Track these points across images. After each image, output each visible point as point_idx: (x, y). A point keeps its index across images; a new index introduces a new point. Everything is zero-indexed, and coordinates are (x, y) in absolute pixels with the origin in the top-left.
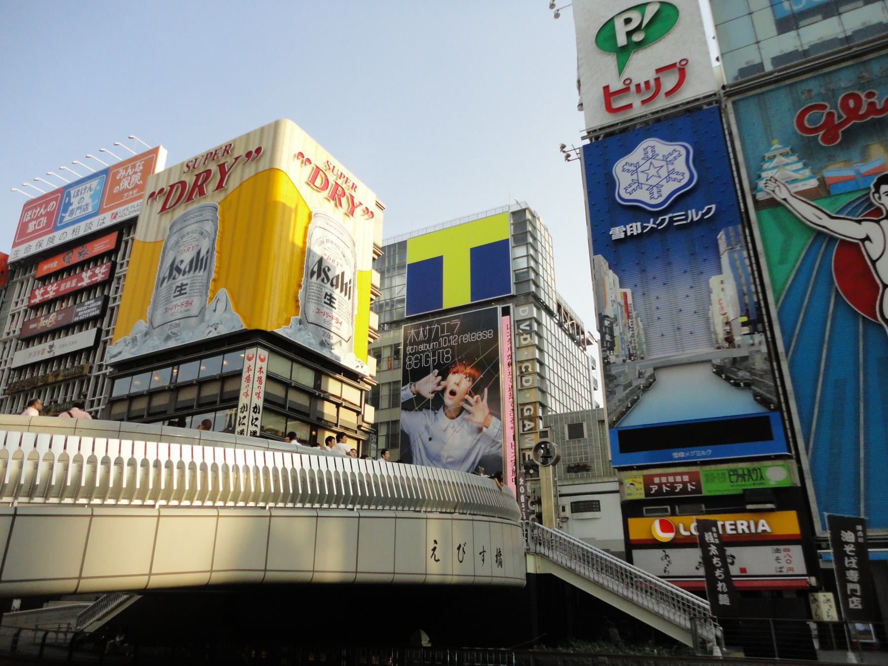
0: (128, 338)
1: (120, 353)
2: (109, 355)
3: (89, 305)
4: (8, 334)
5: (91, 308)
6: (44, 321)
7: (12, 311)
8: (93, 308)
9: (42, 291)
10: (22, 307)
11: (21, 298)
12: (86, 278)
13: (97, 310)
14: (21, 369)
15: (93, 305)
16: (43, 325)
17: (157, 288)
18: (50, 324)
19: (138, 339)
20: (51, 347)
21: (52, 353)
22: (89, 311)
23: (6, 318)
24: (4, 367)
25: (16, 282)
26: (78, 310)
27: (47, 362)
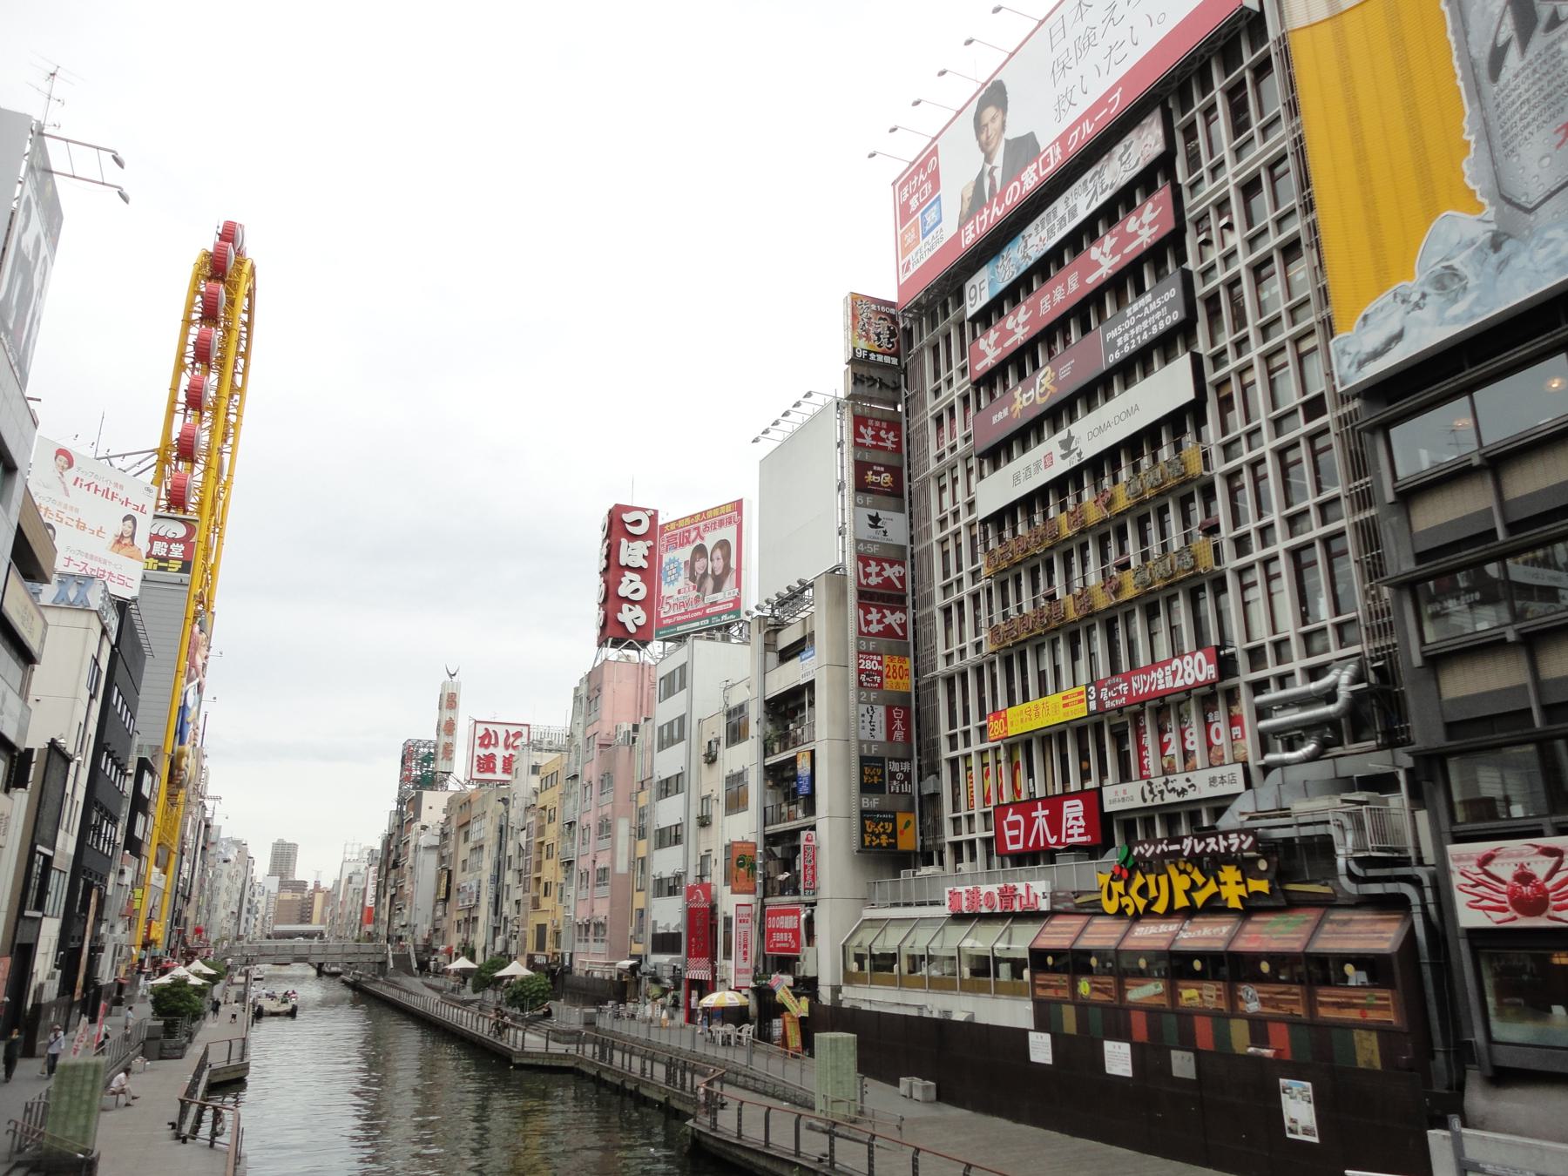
0: (1414, 284)
1: (1398, 337)
2: (1346, 360)
3: (1141, 310)
4: (940, 457)
5: (1148, 316)
6: (1025, 396)
7: (932, 409)
8: (1154, 312)
9: (993, 335)
10: (961, 385)
11: (944, 375)
12: (1104, 258)
13: (1170, 313)
14: (999, 519)
15: (1153, 307)
16: (1025, 404)
17: (1477, 92)
18: (1042, 395)
19: (1464, 270)
20: (1066, 444)
21: (1075, 454)
22: (1145, 324)
23: (924, 426)
24: (957, 526)
25: (921, 350)
26: (1113, 334)
27: (1060, 485)
